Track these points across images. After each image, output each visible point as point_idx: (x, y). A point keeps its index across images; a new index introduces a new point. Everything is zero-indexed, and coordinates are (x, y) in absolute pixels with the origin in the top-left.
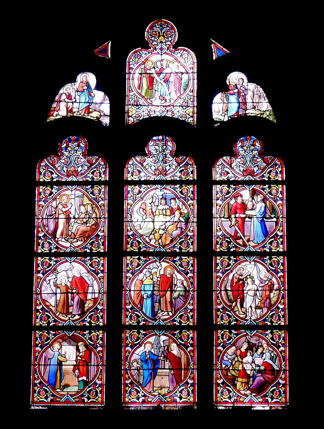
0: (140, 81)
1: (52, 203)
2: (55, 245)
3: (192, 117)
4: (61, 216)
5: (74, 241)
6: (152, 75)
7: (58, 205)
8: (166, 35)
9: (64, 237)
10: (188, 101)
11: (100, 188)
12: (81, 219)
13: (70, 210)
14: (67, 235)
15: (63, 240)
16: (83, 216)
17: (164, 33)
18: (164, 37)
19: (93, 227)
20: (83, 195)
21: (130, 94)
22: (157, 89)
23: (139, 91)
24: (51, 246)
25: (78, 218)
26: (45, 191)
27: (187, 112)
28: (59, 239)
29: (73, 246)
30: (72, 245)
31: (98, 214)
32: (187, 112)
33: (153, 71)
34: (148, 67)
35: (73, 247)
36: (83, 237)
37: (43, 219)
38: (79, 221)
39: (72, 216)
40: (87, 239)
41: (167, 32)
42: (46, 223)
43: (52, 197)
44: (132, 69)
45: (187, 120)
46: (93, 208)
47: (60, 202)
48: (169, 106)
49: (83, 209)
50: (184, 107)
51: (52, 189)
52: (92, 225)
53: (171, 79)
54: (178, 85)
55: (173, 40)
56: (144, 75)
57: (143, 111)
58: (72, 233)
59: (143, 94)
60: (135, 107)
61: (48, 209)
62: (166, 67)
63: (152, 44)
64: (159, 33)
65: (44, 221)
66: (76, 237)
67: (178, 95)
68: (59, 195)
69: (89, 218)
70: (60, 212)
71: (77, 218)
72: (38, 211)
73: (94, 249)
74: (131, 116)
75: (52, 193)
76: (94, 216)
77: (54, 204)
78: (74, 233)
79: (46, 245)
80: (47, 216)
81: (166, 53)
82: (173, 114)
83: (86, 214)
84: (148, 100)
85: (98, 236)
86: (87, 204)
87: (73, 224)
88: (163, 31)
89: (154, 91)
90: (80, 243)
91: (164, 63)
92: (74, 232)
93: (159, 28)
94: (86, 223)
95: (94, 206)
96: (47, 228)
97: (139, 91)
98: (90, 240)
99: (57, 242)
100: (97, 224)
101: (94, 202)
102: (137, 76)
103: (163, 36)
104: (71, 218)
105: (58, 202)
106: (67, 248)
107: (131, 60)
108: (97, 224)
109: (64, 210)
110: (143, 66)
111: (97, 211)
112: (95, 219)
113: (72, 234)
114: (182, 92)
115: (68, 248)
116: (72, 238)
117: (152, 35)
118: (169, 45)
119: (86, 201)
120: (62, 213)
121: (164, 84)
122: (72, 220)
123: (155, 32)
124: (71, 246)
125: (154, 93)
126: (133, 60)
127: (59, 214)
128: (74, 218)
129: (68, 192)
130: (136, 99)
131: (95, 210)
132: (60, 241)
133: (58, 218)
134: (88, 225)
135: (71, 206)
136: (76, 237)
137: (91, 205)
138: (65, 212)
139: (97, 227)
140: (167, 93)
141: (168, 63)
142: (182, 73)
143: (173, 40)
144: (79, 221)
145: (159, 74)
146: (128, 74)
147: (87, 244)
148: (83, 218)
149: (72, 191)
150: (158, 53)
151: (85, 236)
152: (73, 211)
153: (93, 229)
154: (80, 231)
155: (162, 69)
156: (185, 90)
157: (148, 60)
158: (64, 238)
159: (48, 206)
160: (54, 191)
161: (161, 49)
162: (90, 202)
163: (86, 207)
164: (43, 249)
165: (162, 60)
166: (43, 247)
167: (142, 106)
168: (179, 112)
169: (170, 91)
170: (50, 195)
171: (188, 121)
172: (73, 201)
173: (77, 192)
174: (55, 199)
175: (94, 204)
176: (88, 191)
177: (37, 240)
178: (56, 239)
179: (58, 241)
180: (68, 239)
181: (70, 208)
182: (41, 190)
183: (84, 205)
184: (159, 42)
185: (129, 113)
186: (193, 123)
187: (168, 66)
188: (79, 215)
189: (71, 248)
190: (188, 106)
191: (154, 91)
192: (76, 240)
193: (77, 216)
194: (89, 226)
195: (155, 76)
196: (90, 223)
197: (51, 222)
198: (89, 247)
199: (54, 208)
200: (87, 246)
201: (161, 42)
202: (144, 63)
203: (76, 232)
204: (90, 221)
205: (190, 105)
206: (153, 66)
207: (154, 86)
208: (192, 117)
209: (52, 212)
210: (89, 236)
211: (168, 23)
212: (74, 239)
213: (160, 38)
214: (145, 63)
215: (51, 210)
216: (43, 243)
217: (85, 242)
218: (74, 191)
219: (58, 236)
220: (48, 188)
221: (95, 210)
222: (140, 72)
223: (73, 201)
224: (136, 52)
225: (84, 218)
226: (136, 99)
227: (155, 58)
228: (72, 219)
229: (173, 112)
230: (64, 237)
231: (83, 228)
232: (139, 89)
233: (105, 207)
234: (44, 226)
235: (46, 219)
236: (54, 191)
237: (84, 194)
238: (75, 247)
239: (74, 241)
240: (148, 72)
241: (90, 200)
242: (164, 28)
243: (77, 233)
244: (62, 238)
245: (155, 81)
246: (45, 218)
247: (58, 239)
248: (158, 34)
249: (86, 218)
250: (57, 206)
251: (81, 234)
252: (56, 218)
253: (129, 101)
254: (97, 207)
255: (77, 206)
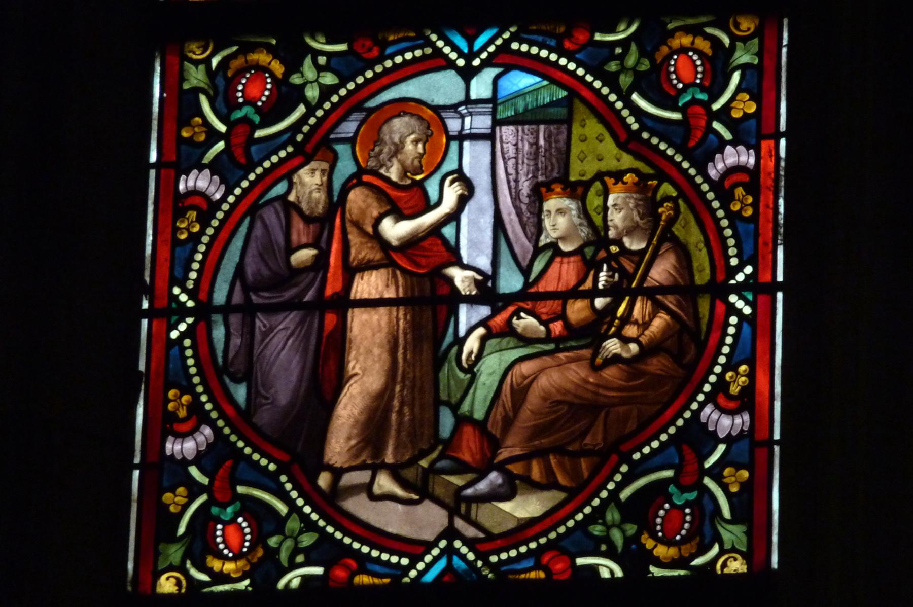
1: (289, 177)
2: (309, 525)
4: (368, 285)
5: (482, 486)
7: (346, 189)
9: (389, 459)
11: (716, 42)
12: (545, 308)
13: (448, 231)
14: (423, 436)
15: (385, 483)
16: (563, 274)
19: (656, 365)
20: (567, 103)
24: (273, 541)
25: (522, 295)
26: (231, 84)
28: (348, 479)
29: (471, 532)
30: (459, 523)
31: (701, 259)
35: (466, 541)
36: (559, 450)
37: (204, 311)
38: (526, 323)
39: (461, 278)
40: (595, 471)
42: (236, 341)
43: (296, 128)
46: (649, 206)
47: (361, 171)
49: (560, 218)
51: (294, 66)
52: (646, 351)
58: (462, 421)
61: (258, 231)
65: (219, 333)
66: (504, 454)
68: (358, 107)
69: (615, 292)
70: (360, 250)
71: (510, 298)
72: (165, 252)
73: (661, 551)
75: (297, 95)
76: (661, 271)
77: (309, 181)
78: (481, 426)
79: (232, 532)
80: (246, 289)
83: (591, 266)
85: (699, 437)
86: (600, 176)
87: (472, 344)
90: (525, 507)
92: (479, 415)
94: (592, 332)
95: (667, 189)
96: (240, 393)
98: (628, 479)
99: (330, 503)
100: (688, 347)
101: (666, 162)
104: (455, 298)
105: (345, 168)
106: (415, 549)
108: (688, 347)
109: (395, 230)
111: (690, 233)
112: (670, 301)
113: (468, 431)
115: (428, 546)
116: (460, 468)
119: (594, 149)
120: (377, 256)
122: (466, 316)
124: (450, 533)
127: (350, 272)
128: (486, 291)
129: (440, 87)
131: (672, 221)
132: (354, 490)
133: (344, 303)
134: (612, 346)
135: (463, 201)
136: (504, 454)
137: (641, 185)
138: (411, 243)
139: (691, 368)
144: (526, 323)
147: (598, 514)
148: (565, 296)
149: (468, 74)
151: (573, 441)
152: (474, 240)
153: (658, 380)
154: (533, 399)
158: (395, 473)
159: (254, 210)
160: (311, 78)
162: (627, 161)
163: (593, 200)
164: (203, 568)
166: (200, 546)
170: (271, 115)
172: (474, 159)
173: (521, 81)
174: (316, 146)
175: (662, 177)
176: (613, 67)
177: (152, 490)
178: (324, 480)
179: (336, 493)
180: (427, 472)
181: (454, 217)
182: (196, 77)
183: (577, 190)
188: (525, 271)
189: (450, 551)
192: (494, 477)
193: (510, 281)
194: (616, 359)
196: (631, 331)
197: (278, 339)
198: (617, 536)
199: (308, 219)
200: (597, 530)
203: (498, 413)
204: (627, 319)
209: (291, 250)
210: (615, 451)
212: (482, 475)
215: (280, 239)
216: (203, 522)
217: (577, 493)
218: (490, 74)
219: (338, 446)
220: (263, 58)
221: (672, 221)
223: (474, 159)
225: (574, 293)
228: (463, 310)
230: (389, 459)
231: (561, 376)
233: (766, 197)
234: (216, 373)
235: (235, 319)
236: (311, 78)
237: (573, 94)
238: (490, 536)
239: (482, 486)
241: (627, 141)
243: (508, 423)
244: (375, 469)
246: (227, 310)
247: (337, 473)
249: (595, 293)
250: (336, 204)
251: (537, 432)
252: (322, 305)
254: (689, 193)
255: (516, 198)
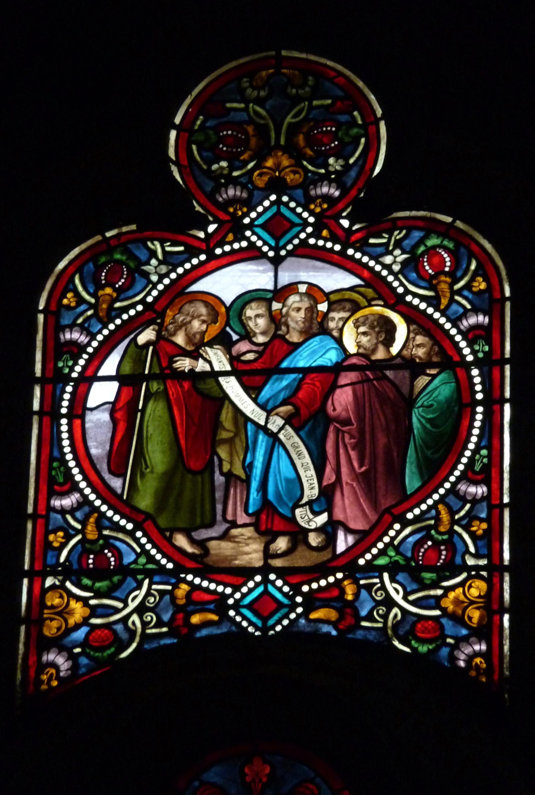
0: (122, 426)
3: (486, 631)
6: (208, 385)
8: (310, 142)
10: (451, 532)
17: (293, 129)
18: (297, 157)
21: (56, 503)
22: (239, 471)
23: (116, 483)
27: (448, 603)
32: (448, 603)
33: (218, 359)
34: (180, 339)
41: (319, 123)
44: (75, 350)
45: (445, 651)
48: (323, 570)
50: (428, 576)
53: (343, 400)
54: (382, 440)
55: (353, 173)
56: (155, 386)
57: (141, 610)
59: (145, 502)
60: (86, 581)
62: (308, 335)
63: (211, 197)
64: (262, 131)
67: (386, 502)
74: (58, 643)
81: (304, 251)
82: (350, 620)
84: (181, 541)
88: (289, 119)
89: (219, 480)
91: (296, 309)
93: (259, 101)
97: (116, 483)
102: (103, 393)
103: (292, 150)
107: (69, 299)
110: (147, 335)
114: (412, 482)
117: (214, 148)
118: (326, 198)
121: (289, 436)
123: (238, 126)
125: (219, 495)
126: (81, 301)
130: (92, 534)
140: (311, 491)
141: (323, 307)
142: (412, 367)
143: (353, 173)
145: (252, 378)
146: (42, 381)
150: (252, 254)
155: (279, 346)
156: (433, 471)
157: (182, 293)
161: (277, 226)
165: (281, 293)
167: (134, 573)
168: (389, 603)
169: (329, 477)
171: (453, 659)
184: (260, 182)
185: (41, 622)
186: (488, 672)
187: (317, 327)
190: (452, 568)
191: (219, 480)
195: (232, 387)
201: (277, 185)
202: (153, 314)
205: (471, 562)
206: (214, 330)
207: (223, 452)
208: (486, 631)
211: (320, 72)
213: (270, 163)
214: (162, 315)
222: (127, 369)
224: (107, 247)
226: (92, 534)
227: (228, 283)
229: (348, 610)
232: (117, 467)
240: (184, 364)
242: (297, 100)
245: (226, 417)
248: (253, 142)
253: (48, 545)
